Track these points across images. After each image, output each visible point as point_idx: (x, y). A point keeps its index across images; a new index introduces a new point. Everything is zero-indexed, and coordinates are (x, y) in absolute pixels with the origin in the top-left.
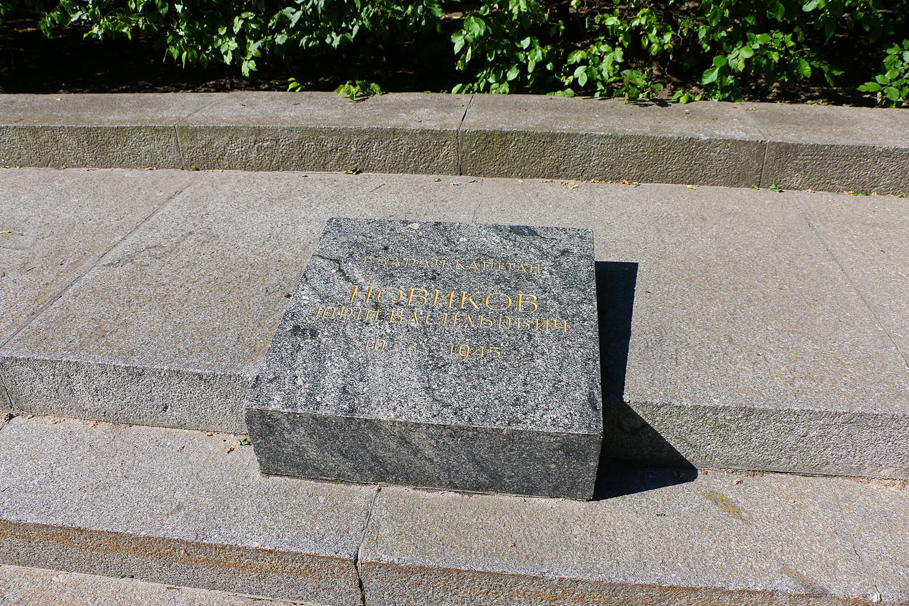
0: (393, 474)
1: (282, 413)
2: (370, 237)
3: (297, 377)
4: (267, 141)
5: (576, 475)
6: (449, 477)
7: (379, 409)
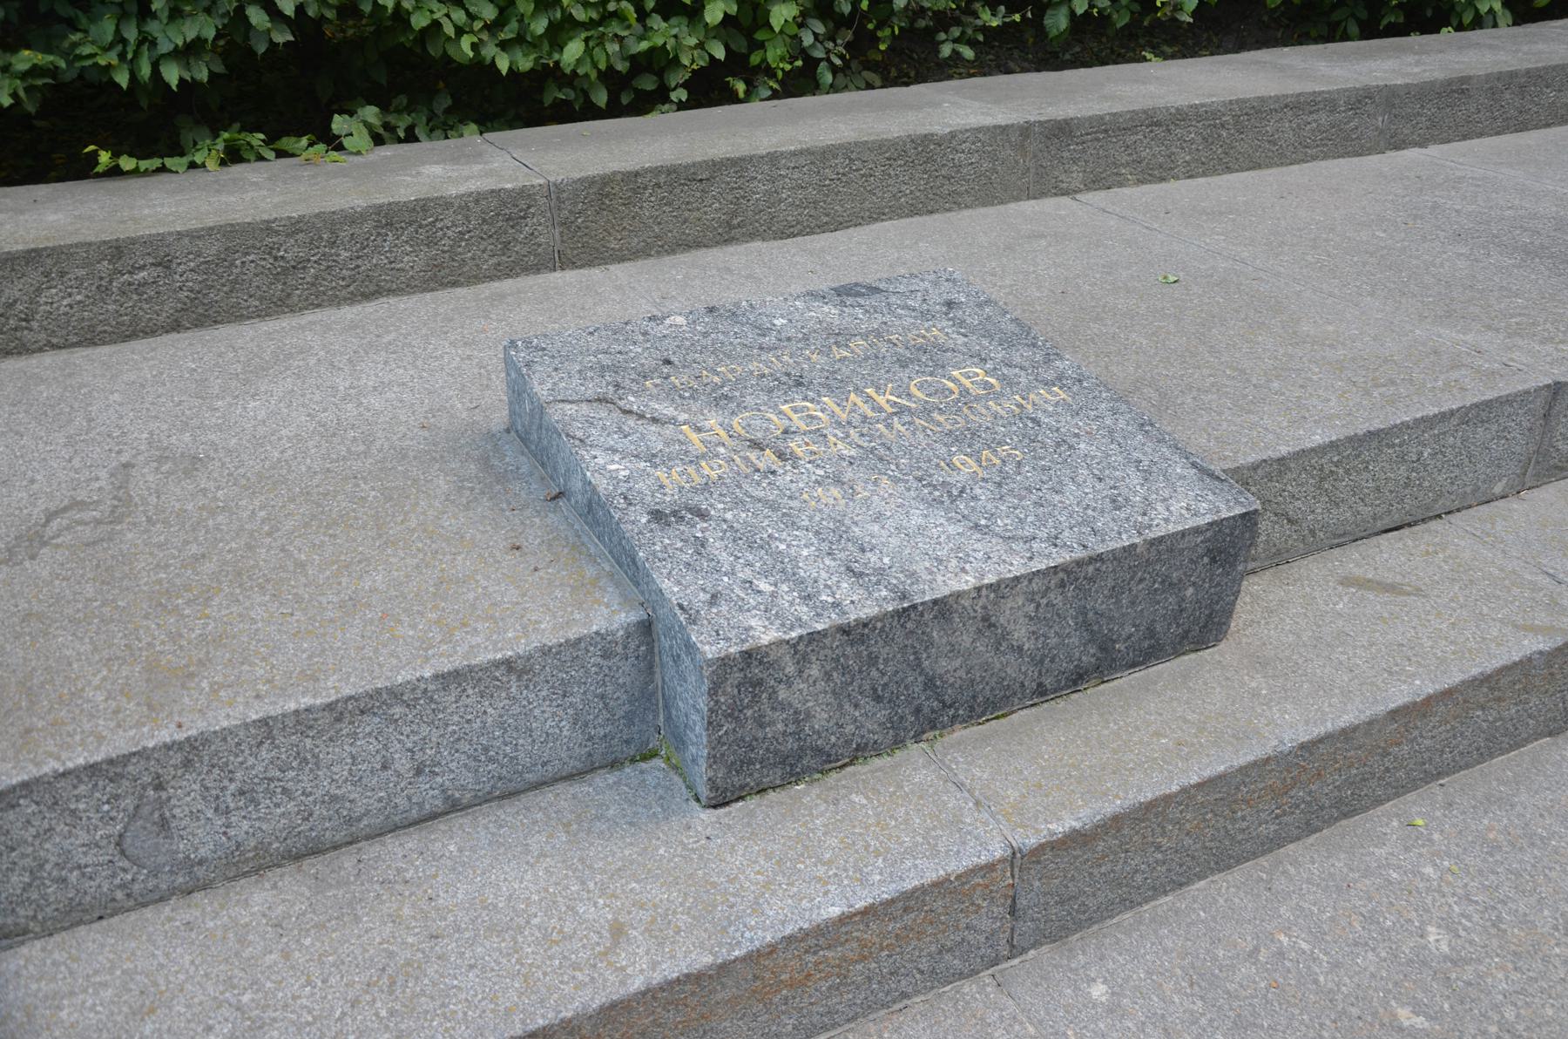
0: (950, 706)
1: (788, 642)
2: (620, 352)
3: (751, 582)
4: (142, 268)
5: (1216, 598)
6: (1040, 674)
7: (940, 578)
